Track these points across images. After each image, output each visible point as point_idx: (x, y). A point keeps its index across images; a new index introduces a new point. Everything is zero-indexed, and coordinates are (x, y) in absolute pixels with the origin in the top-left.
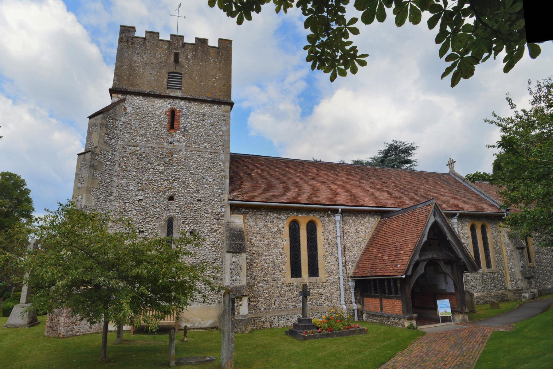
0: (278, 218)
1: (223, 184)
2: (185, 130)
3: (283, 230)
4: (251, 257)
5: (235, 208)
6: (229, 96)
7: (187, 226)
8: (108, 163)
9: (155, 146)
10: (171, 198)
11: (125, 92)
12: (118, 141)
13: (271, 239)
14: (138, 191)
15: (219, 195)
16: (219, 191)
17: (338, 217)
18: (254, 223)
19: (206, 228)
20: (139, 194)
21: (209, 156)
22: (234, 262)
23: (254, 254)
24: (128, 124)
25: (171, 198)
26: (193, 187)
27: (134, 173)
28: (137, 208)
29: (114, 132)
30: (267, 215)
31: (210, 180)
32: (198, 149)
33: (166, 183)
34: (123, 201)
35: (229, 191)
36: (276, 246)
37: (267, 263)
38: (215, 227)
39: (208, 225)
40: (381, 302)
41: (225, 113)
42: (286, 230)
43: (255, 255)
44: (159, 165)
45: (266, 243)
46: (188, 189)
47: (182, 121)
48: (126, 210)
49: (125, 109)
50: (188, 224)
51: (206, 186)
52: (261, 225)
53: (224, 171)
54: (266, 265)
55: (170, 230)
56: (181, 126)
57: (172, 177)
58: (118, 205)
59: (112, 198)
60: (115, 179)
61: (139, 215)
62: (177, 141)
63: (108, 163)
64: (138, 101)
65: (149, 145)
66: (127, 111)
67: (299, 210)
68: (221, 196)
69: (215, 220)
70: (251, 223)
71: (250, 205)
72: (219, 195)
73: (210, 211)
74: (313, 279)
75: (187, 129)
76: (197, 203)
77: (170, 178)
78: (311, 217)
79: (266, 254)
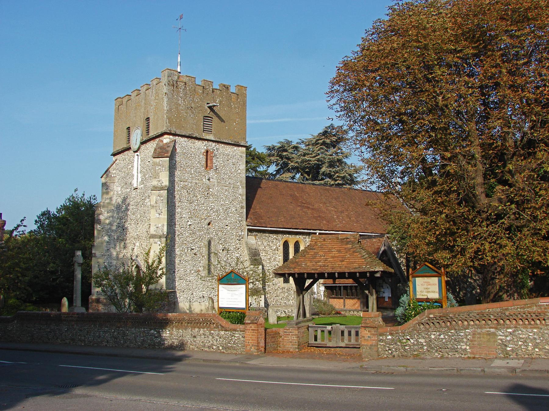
1: (242, 213)
6: (245, 139)
9: (197, 182)
10: (209, 224)
32: (225, 185)
33: (206, 212)
36: (275, 260)
42: (281, 248)
45: (269, 257)
52: (265, 244)
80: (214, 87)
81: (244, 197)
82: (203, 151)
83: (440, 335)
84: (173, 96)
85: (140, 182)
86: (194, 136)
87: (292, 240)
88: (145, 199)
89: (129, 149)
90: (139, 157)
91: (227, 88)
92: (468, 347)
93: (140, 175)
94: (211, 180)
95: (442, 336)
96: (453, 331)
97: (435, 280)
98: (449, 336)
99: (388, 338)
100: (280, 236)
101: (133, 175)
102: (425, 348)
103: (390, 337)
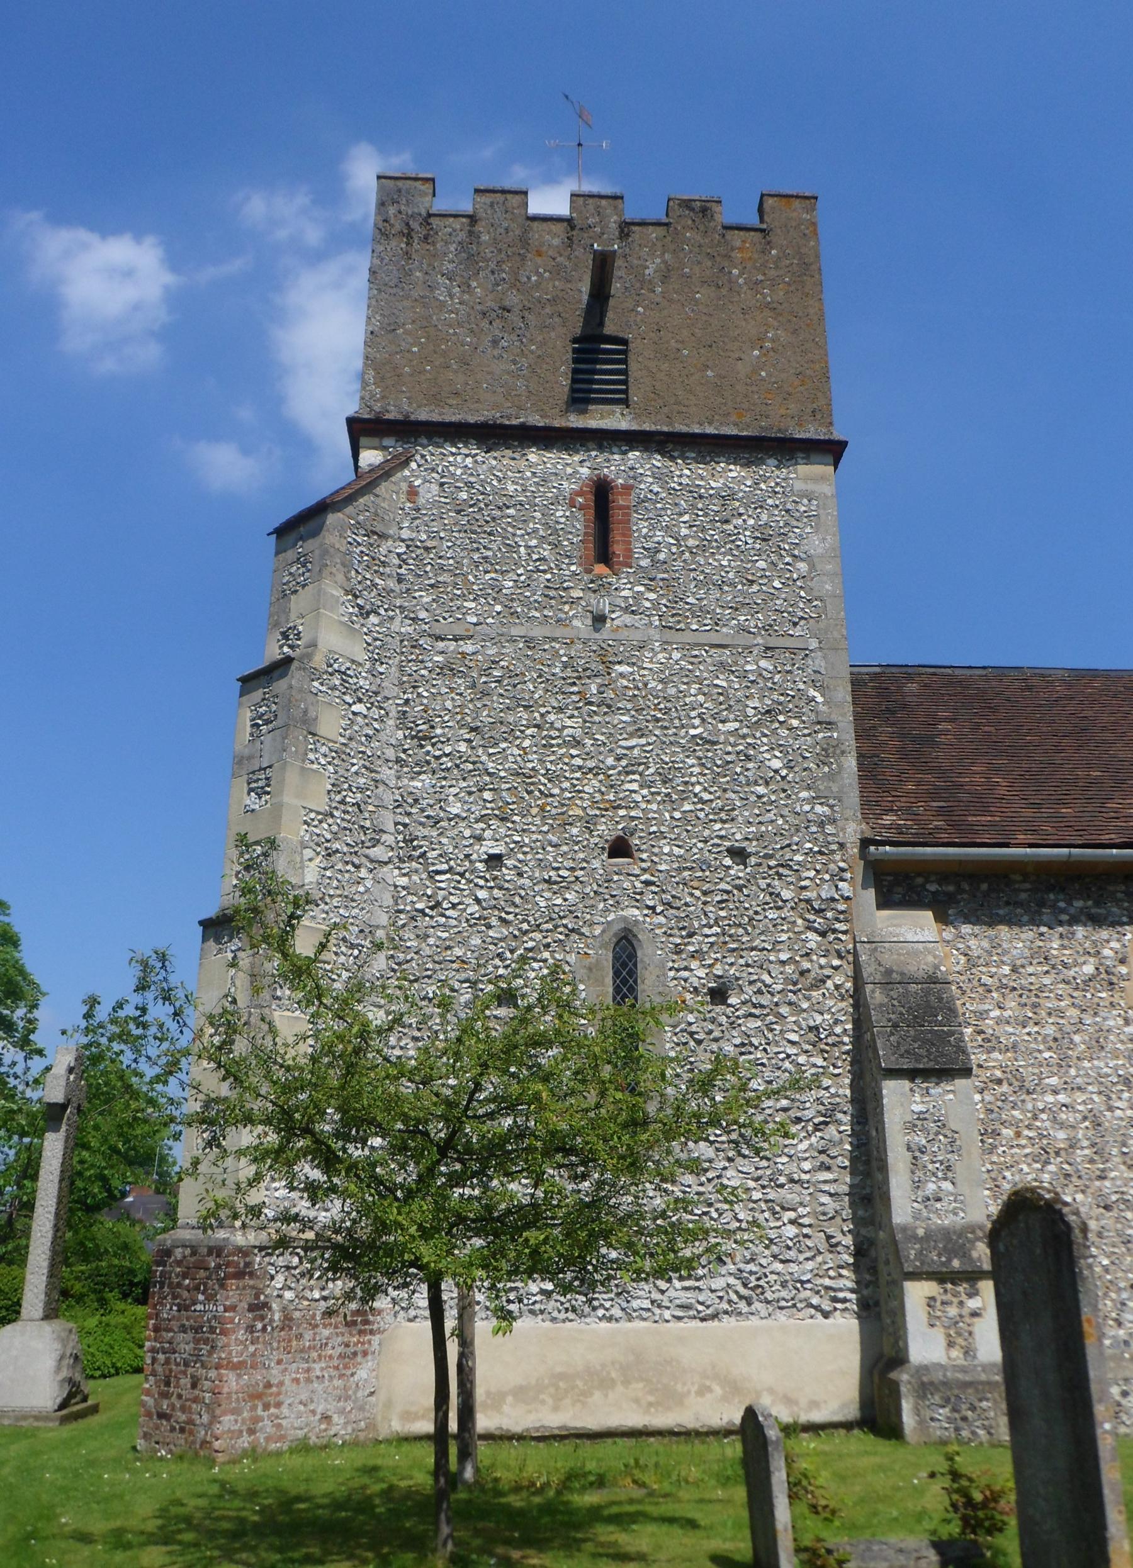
1: (831, 777)
3: (1124, 970)
4: (988, 1098)
5: (896, 885)
6: (822, 414)
7: (694, 964)
8: (357, 708)
9: (537, 632)
10: (620, 848)
11: (409, 431)
12: (392, 618)
13: (1073, 1012)
14: (482, 818)
15: (822, 825)
16: (819, 809)
18: (986, 944)
19: (775, 969)
20: (488, 834)
21: (763, 663)
22: (921, 1117)
23: (999, 1082)
24: (427, 549)
25: (620, 848)
26: (706, 796)
27: (463, 747)
28: (482, 894)
29: (375, 585)
30: (1042, 904)
31: (776, 764)
32: (715, 638)
33: (592, 785)
34: (426, 865)
35: (865, 803)
36: (1097, 1045)
37: (1062, 1125)
38: (815, 965)
39: (784, 956)
41: (810, 487)
43: (1005, 1088)
44: (560, 710)
45: (1050, 1030)
46: (687, 807)
48: (438, 904)
49: (413, 493)
50: (697, 955)
51: (761, 790)
53: (829, 725)
54: (1061, 1135)
55: (624, 982)
56: (638, 551)
57: (618, 759)
58: (404, 881)
59: (378, 852)
60: (387, 773)
61: (494, 922)
62: (626, 610)
63: (357, 708)
64: (462, 460)
65: (515, 631)
66: (421, 501)
68: (829, 829)
69: (811, 935)
70: (973, 943)
71: (961, 863)
72: (822, 825)
73: (786, 894)
75: (662, 556)
76: (728, 862)
77: (610, 761)
79: (1054, 1081)
80: (628, 216)
84: (409, 273)
91: (702, 210)
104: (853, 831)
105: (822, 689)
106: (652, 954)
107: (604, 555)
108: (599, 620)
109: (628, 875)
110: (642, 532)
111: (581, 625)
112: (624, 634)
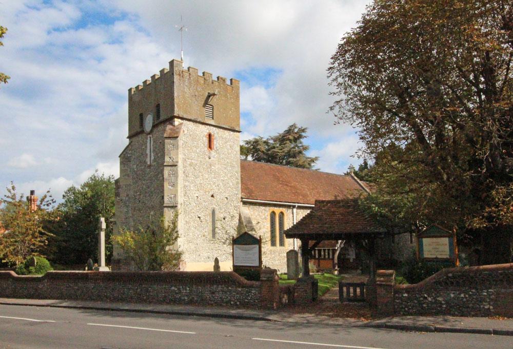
0: (265, 210)
2: (217, 150)
5: (245, 203)
6: (238, 125)
10: (212, 196)
17: (295, 210)
25: (212, 196)
27: (193, 178)
40: (260, 262)
42: (269, 218)
47: (215, 143)
50: (222, 213)
52: (256, 213)
53: (238, 179)
58: (185, 199)
67: (275, 205)
74: (282, 248)
78: (281, 209)
81: (239, 174)
82: (206, 134)
83: (460, 294)
85: (153, 160)
86: (199, 120)
87: (278, 210)
88: (158, 175)
89: (142, 132)
90: (152, 139)
92: (491, 307)
93: (152, 154)
94: (212, 158)
95: (462, 295)
96: (474, 291)
97: (446, 240)
98: (470, 295)
99: (404, 295)
100: (267, 208)
101: (147, 155)
102: (445, 306)
103: (406, 295)
104: (240, 196)
105: (237, 174)
106: (217, 212)
107: (210, 147)
108: (210, 158)
109: (214, 200)
110: (215, 143)
111: (207, 159)
112: (213, 161)
